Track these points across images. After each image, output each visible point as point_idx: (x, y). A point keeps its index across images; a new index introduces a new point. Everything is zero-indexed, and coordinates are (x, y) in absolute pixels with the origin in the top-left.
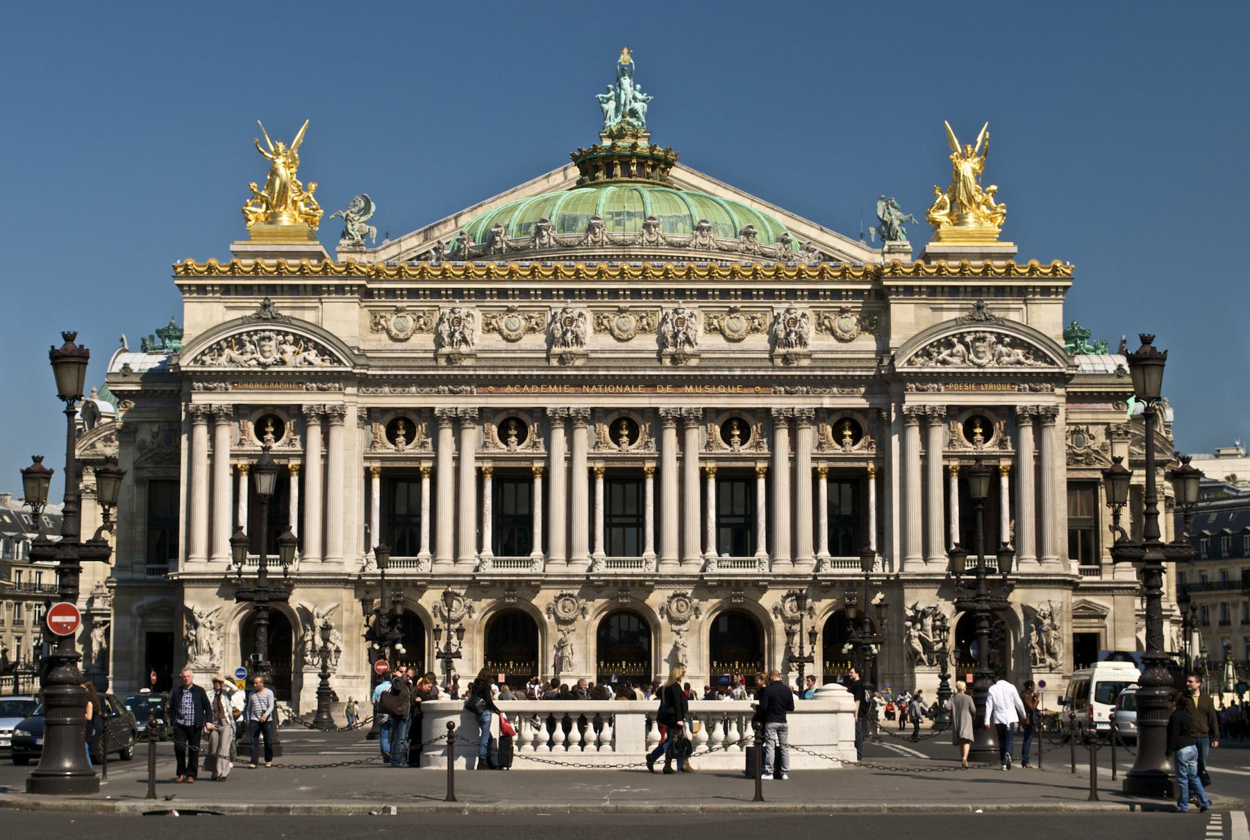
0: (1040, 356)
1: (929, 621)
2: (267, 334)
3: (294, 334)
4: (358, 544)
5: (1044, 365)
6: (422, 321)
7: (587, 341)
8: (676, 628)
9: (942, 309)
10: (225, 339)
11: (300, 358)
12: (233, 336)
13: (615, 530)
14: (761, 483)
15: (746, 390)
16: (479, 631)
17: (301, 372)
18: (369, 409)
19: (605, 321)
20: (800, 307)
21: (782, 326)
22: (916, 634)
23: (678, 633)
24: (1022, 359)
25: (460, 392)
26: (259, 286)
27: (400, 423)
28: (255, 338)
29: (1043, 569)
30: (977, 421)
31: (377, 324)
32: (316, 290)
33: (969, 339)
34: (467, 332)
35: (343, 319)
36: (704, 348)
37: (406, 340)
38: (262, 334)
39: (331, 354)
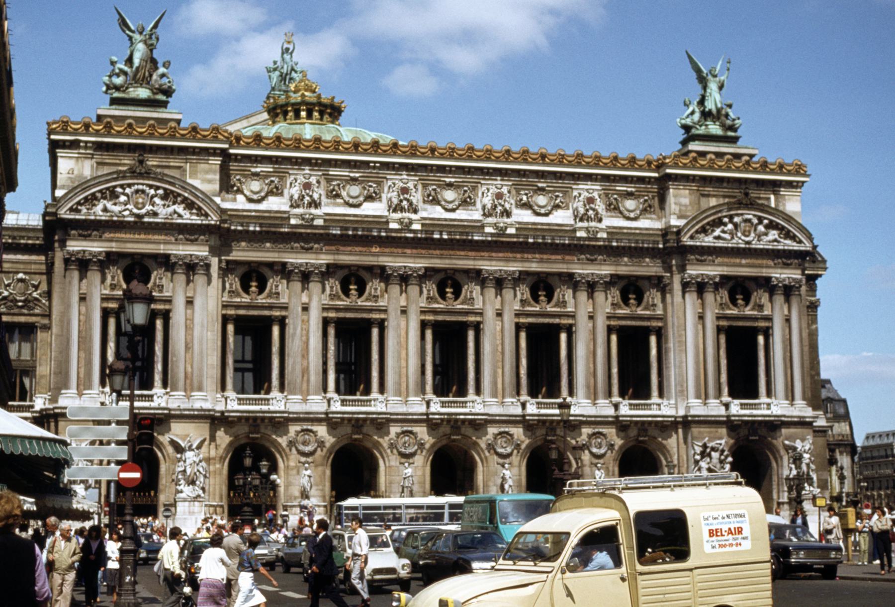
0: (788, 235)
1: (715, 455)
2: (140, 187)
3: (165, 189)
5: (795, 244)
9: (708, 196)
10: (100, 191)
12: (107, 189)
18: (228, 262)
22: (707, 466)
23: (503, 466)
25: (311, 248)
27: (253, 276)
28: (128, 191)
29: (796, 413)
30: (739, 289)
33: (736, 219)
34: (316, 196)
35: (203, 179)
37: (259, 201)
38: (136, 187)
39: (199, 209)
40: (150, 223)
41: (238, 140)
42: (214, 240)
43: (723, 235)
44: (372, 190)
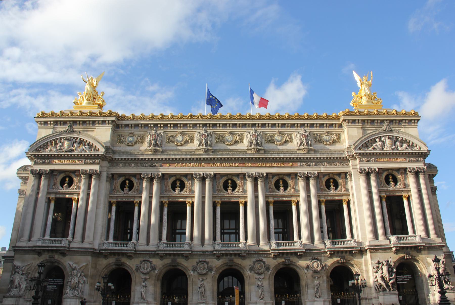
3: (80, 139)
4: (101, 236)
6: (139, 138)
7: (213, 145)
8: (258, 277)
10: (51, 141)
11: (81, 148)
12: (54, 140)
13: (225, 235)
15: (286, 165)
16: (158, 280)
17: (81, 155)
18: (113, 175)
19: (221, 138)
20: (308, 130)
21: (299, 138)
22: (380, 276)
23: (259, 279)
24: (408, 148)
26: (70, 121)
27: (128, 182)
31: (120, 139)
32: (94, 122)
33: (383, 139)
36: (265, 148)
37: (132, 145)
40: (71, 155)
41: (122, 118)
42: (105, 164)
43: (376, 147)
44: (188, 138)
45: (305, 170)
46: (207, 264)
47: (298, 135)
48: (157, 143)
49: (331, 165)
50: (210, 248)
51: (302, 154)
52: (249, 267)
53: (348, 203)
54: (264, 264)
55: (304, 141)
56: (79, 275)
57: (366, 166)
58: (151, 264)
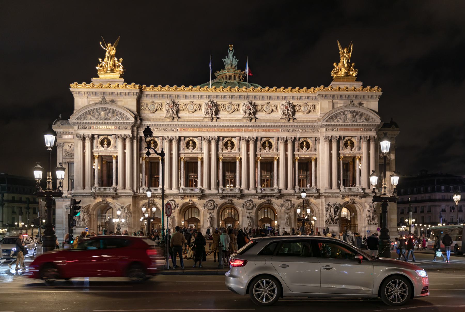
9: (337, 103)
10: (89, 111)
11: (115, 118)
12: (91, 110)
14: (276, 163)
33: (346, 113)
45: (285, 135)
46: (214, 203)
47: (282, 107)
48: (173, 112)
49: (305, 131)
50: (216, 192)
51: (284, 123)
52: (242, 205)
53: (316, 160)
54: (252, 203)
55: (286, 112)
56: (126, 212)
57: (331, 134)
58: (175, 203)
